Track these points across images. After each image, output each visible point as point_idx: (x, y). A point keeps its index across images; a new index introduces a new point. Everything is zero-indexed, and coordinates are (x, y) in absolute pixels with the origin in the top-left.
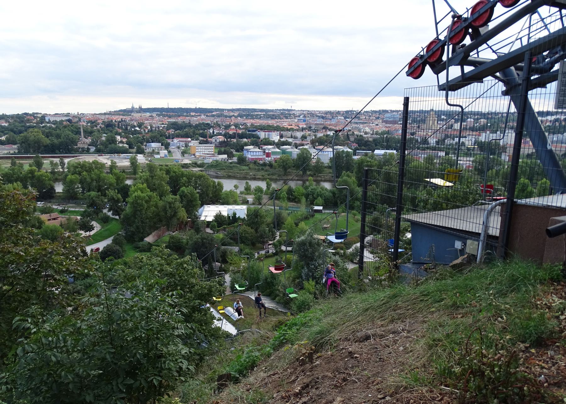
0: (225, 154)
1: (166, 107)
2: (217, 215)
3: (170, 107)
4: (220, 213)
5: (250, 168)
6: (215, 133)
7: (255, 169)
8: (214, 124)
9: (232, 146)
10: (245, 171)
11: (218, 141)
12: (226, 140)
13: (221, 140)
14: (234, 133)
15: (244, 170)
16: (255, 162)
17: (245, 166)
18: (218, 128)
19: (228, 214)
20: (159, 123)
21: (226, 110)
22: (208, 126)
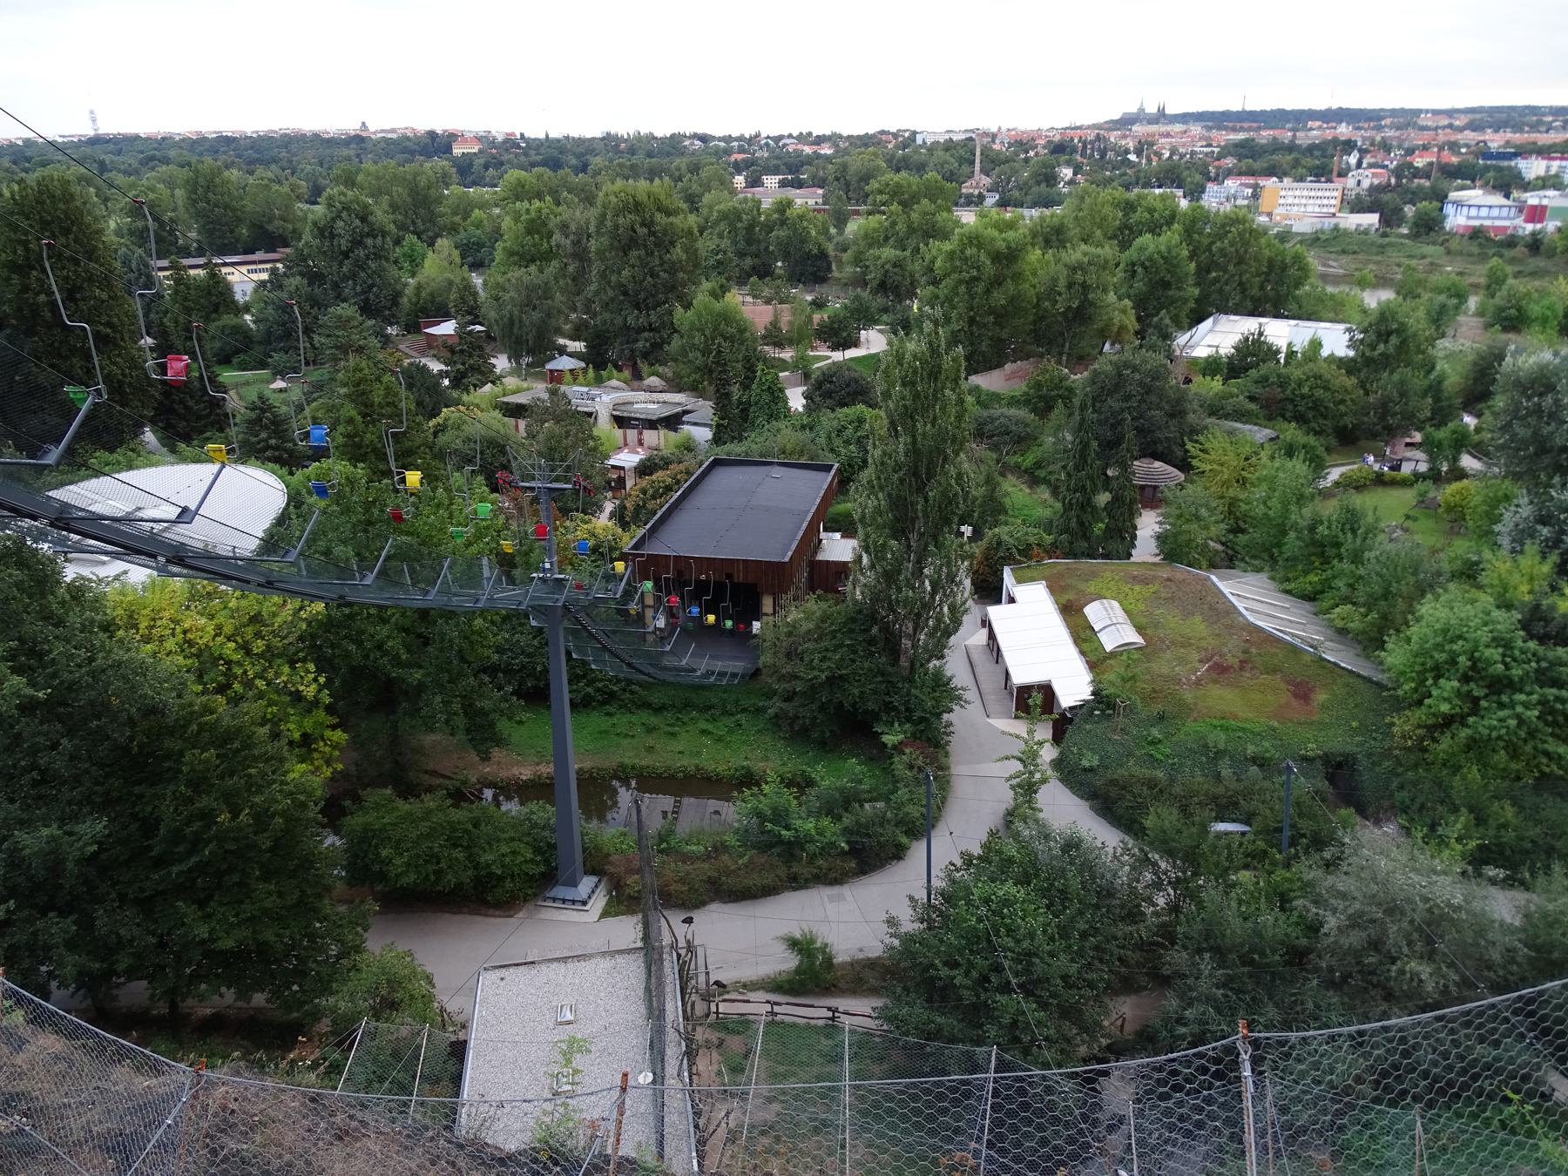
0: (1371, 210)
1: (1236, 107)
2: (1247, 339)
3: (1248, 108)
4: (1261, 334)
5: (1449, 252)
6: (1364, 165)
7: (1470, 255)
8: (1372, 144)
9: (1410, 196)
10: (1427, 261)
11: (1366, 184)
12: (1393, 181)
13: (1376, 182)
14: (1431, 164)
15: (1424, 257)
16: (1476, 234)
17: (1434, 243)
18: (1382, 153)
19: (1290, 345)
20: (1193, 141)
21: (1427, 111)
22: (1349, 146)
